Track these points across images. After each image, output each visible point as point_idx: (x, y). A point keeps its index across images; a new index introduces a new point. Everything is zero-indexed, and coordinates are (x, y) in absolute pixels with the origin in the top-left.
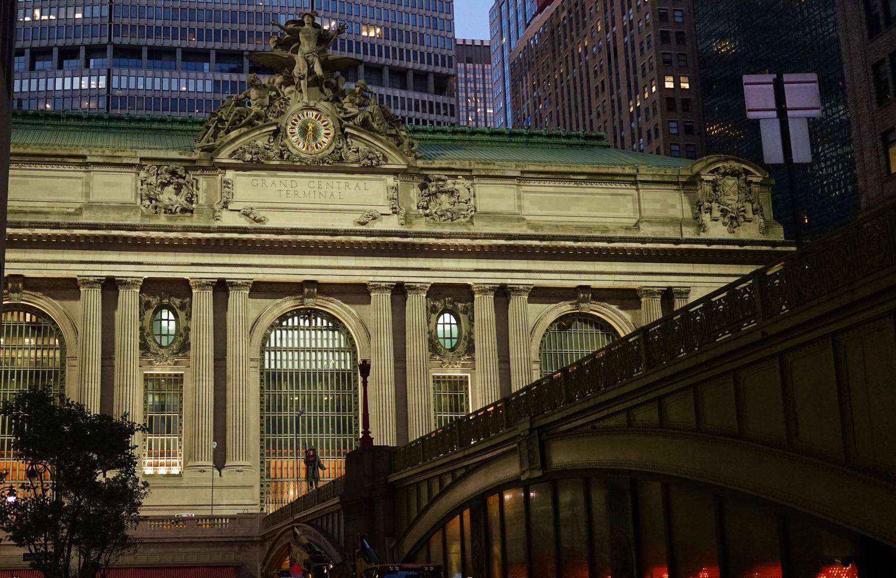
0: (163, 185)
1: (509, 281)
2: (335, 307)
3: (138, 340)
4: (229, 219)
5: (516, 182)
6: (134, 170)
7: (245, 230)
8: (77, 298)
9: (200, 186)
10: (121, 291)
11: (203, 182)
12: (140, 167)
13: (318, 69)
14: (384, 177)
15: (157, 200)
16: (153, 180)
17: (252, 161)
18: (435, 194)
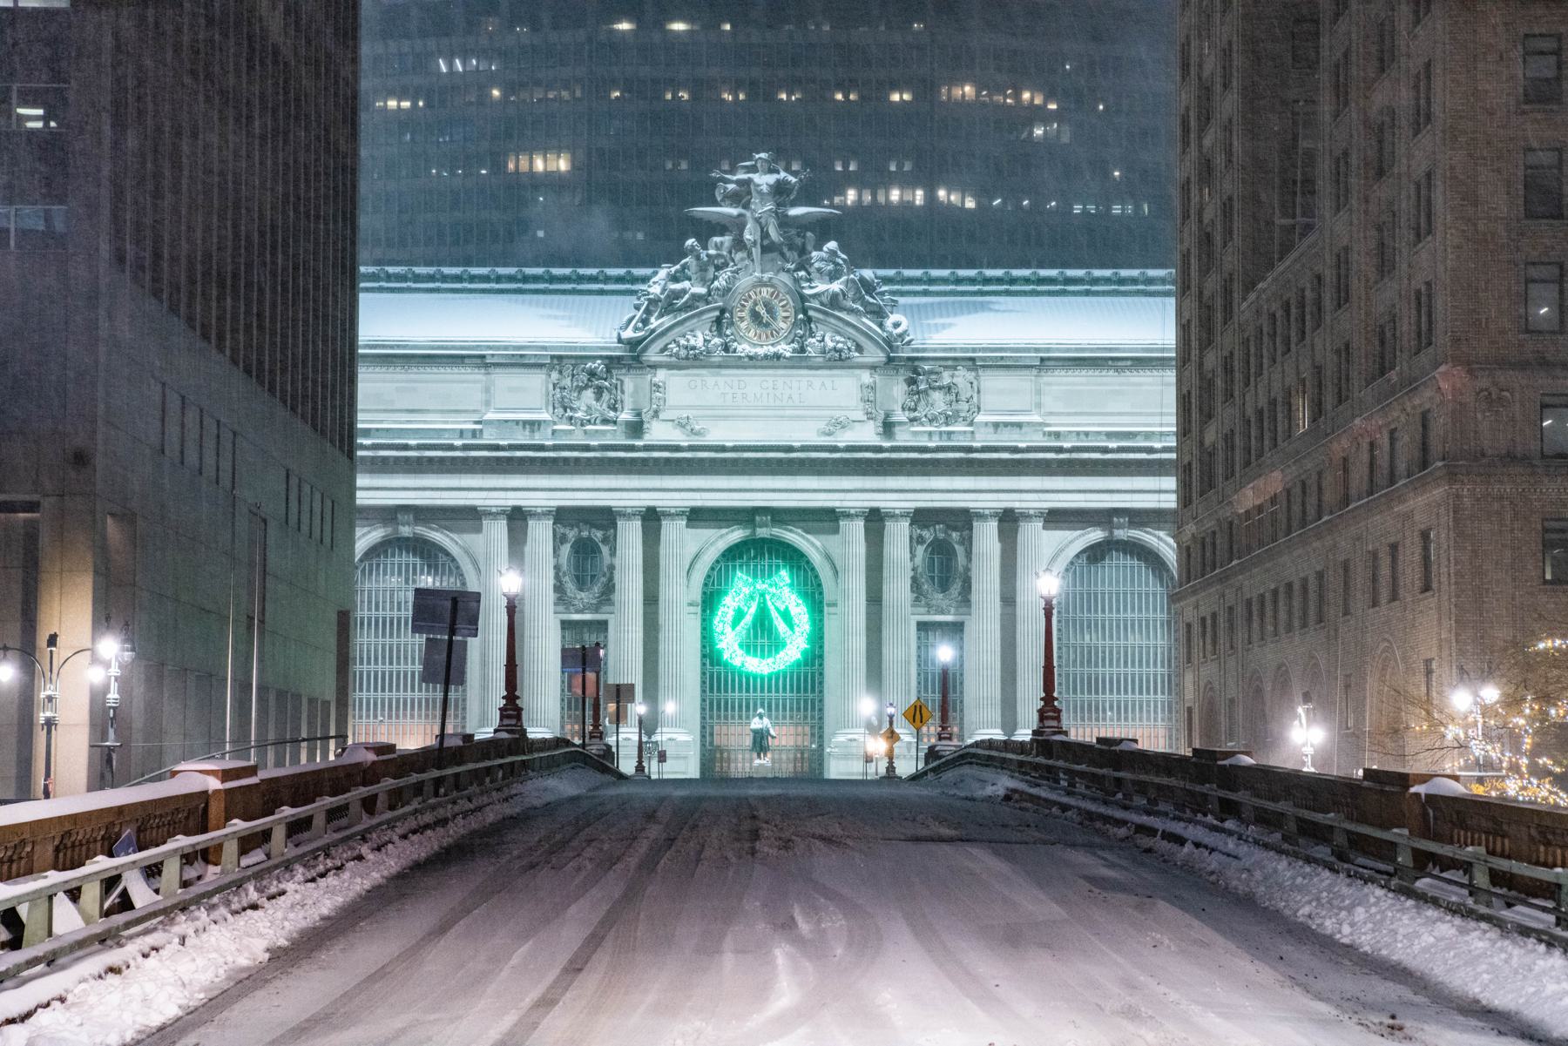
0: (581, 389)
1: (1017, 505)
2: (794, 536)
3: (551, 582)
4: (659, 433)
5: (1035, 372)
6: (544, 370)
7: (678, 449)
8: (479, 530)
9: (626, 388)
10: (531, 523)
11: (629, 383)
12: (551, 367)
13: (774, 234)
14: (857, 372)
15: (572, 409)
16: (567, 382)
17: (687, 358)
18: (925, 391)
